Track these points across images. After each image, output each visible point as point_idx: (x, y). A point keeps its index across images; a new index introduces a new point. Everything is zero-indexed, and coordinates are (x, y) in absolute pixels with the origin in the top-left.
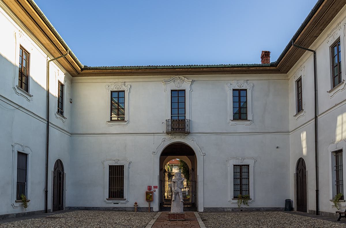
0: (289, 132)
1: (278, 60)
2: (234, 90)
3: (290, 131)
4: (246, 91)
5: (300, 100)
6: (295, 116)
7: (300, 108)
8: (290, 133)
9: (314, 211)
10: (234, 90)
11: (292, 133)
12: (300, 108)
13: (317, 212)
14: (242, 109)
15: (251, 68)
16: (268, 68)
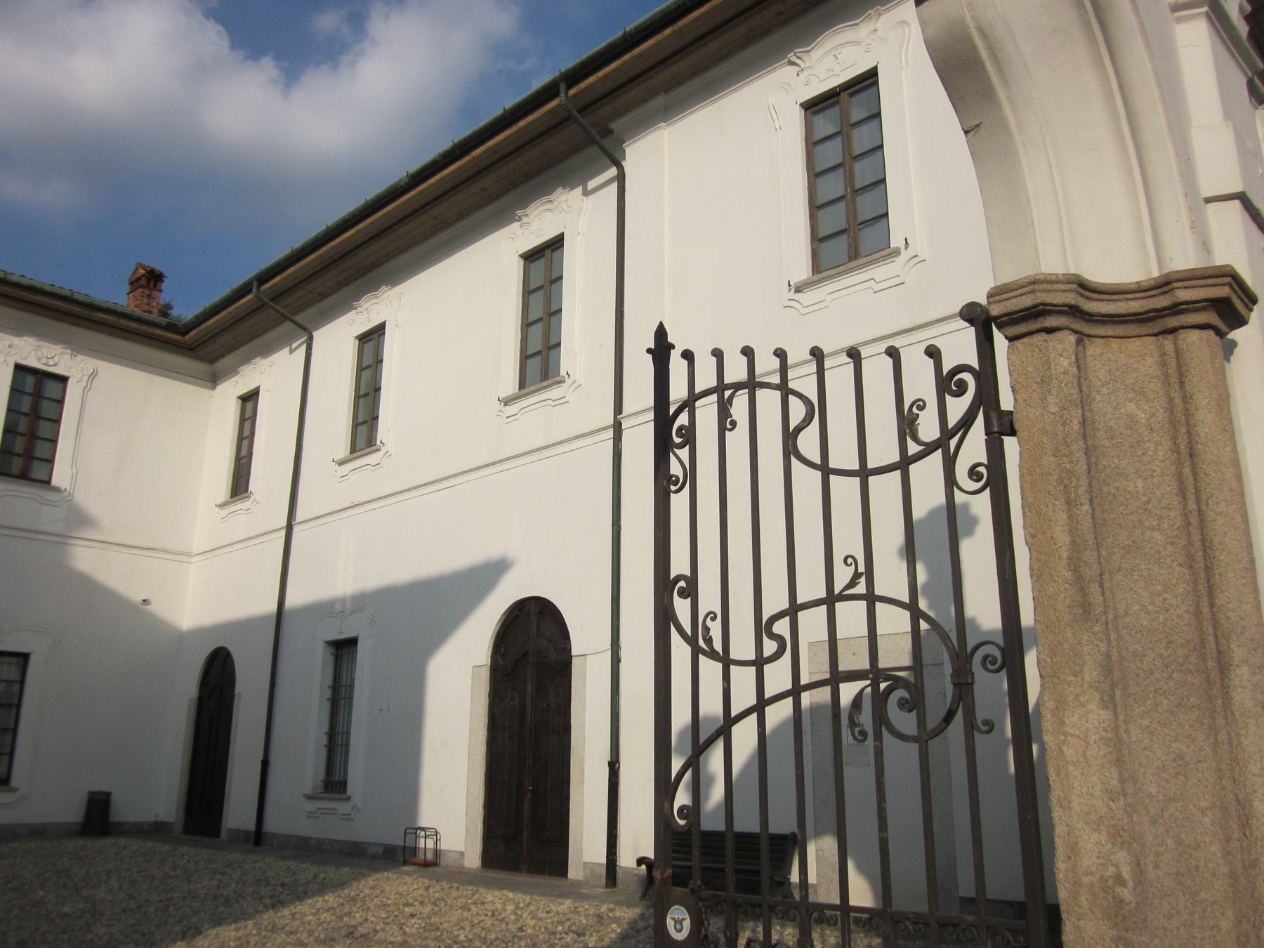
0: (189, 555)
1: (197, 317)
2: (19, 368)
3: (195, 551)
4: (61, 385)
5: (244, 461)
6: (222, 506)
7: (240, 485)
8: (194, 559)
9: (247, 832)
10: (19, 368)
11: (200, 558)
12: (240, 485)
13: (258, 837)
14: (39, 444)
15: (101, 315)
16: (158, 332)
